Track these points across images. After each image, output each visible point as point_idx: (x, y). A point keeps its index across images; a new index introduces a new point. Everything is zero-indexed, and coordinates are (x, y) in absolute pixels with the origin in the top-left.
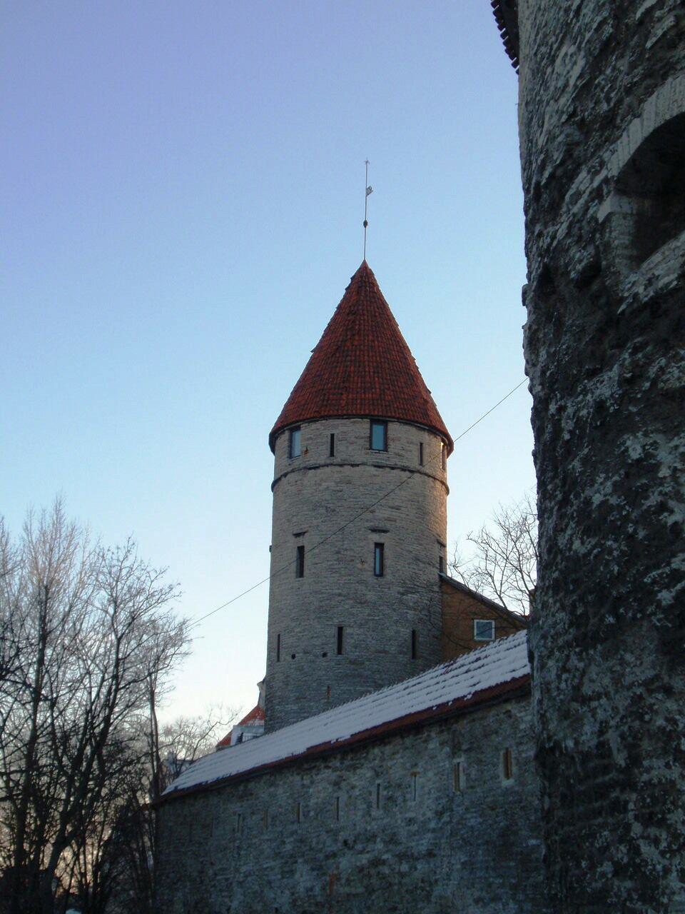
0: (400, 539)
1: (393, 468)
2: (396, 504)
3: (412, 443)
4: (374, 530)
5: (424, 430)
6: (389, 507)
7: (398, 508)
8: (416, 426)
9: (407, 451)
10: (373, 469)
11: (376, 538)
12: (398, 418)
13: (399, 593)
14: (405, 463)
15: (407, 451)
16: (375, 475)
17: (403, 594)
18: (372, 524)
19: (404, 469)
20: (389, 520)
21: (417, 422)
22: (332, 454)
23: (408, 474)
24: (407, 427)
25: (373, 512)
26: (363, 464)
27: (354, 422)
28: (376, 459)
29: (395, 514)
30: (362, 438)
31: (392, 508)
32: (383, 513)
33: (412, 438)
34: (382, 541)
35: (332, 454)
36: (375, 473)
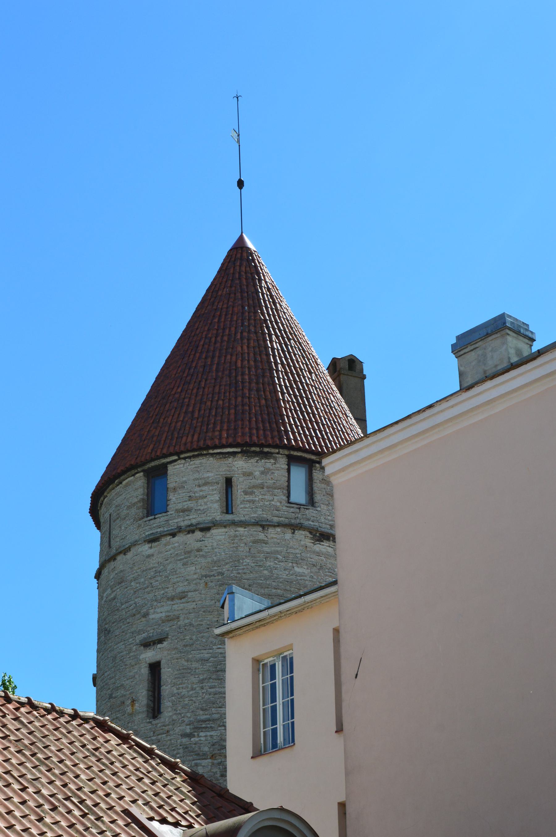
0: (185, 646)
1: (174, 535)
2: (179, 590)
3: (206, 484)
4: (147, 644)
5: (234, 454)
6: (168, 599)
7: (182, 596)
8: (212, 455)
9: (197, 499)
10: (147, 546)
11: (150, 655)
12: (178, 454)
13: (185, 735)
14: (194, 519)
15: (197, 499)
16: (149, 556)
17: (190, 736)
18: (144, 635)
19: (191, 530)
20: (169, 619)
21: (208, 448)
22: (110, 546)
23: (198, 534)
24: (197, 461)
25: (146, 615)
26: (135, 544)
27: (127, 485)
28: (151, 529)
29: (178, 606)
30: (134, 504)
31: (172, 599)
32: (158, 613)
33: (210, 474)
34: (157, 658)
35: (110, 546)
36: (150, 552)
